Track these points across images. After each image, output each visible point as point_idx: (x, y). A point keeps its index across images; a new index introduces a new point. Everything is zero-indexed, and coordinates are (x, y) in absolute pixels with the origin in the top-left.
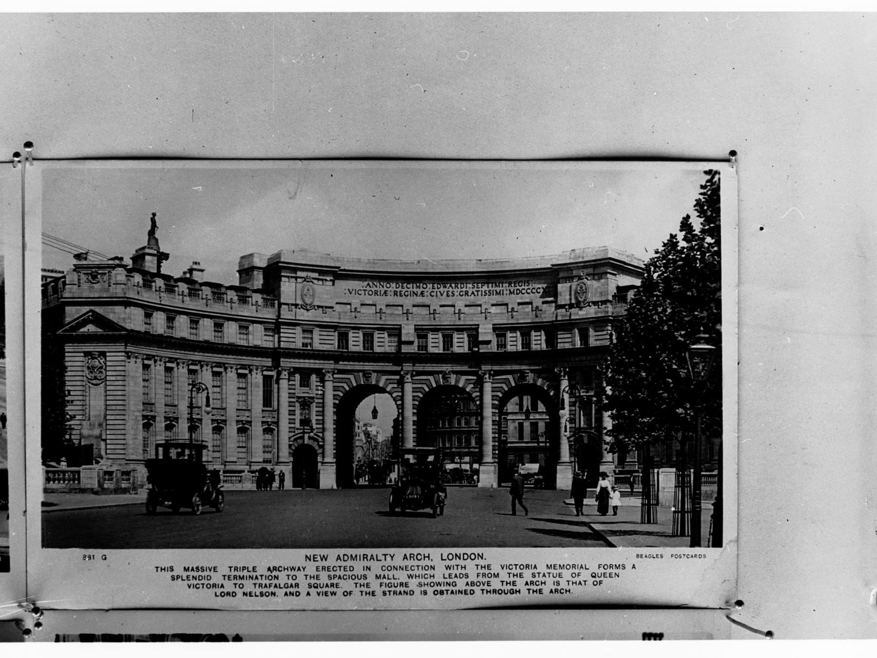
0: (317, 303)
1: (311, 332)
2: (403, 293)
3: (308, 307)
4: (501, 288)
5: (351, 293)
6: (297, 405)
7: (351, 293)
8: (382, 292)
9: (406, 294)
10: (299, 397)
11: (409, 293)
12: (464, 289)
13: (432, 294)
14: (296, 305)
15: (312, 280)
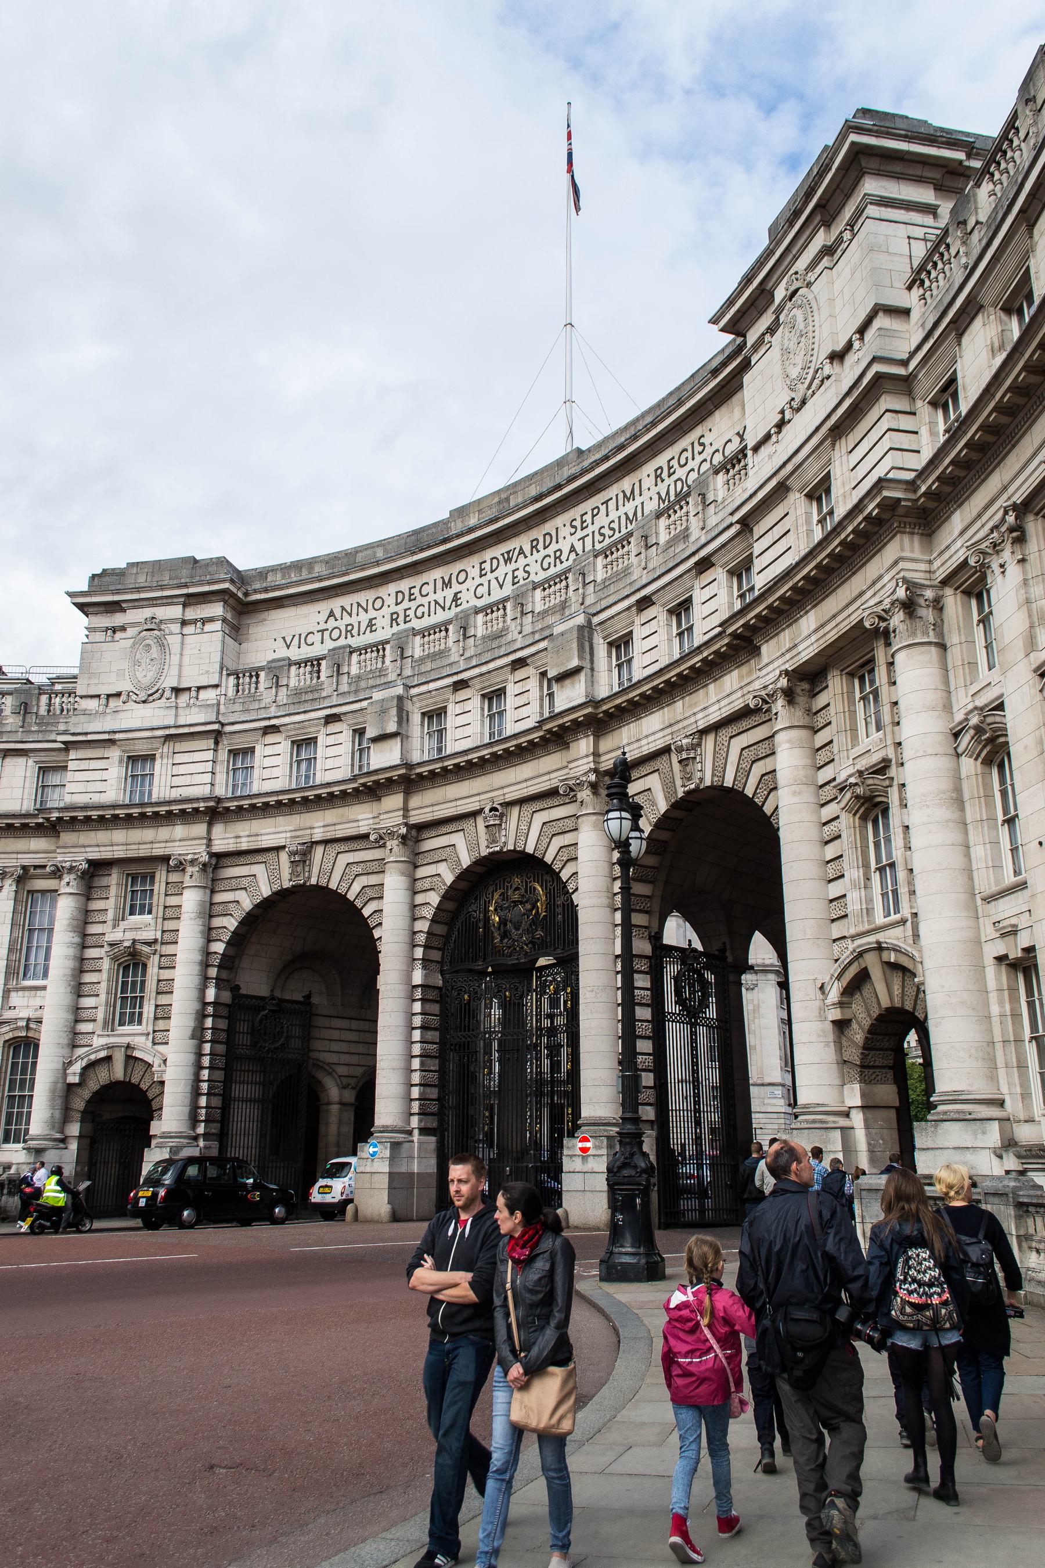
0: (170, 681)
1: (152, 758)
2: (411, 613)
3: (143, 696)
4: (638, 500)
5: (288, 647)
6: (106, 964)
7: (288, 647)
8: (362, 629)
9: (419, 614)
10: (111, 945)
11: (426, 610)
12: (554, 547)
13: (481, 591)
14: (118, 695)
15: (163, 627)
